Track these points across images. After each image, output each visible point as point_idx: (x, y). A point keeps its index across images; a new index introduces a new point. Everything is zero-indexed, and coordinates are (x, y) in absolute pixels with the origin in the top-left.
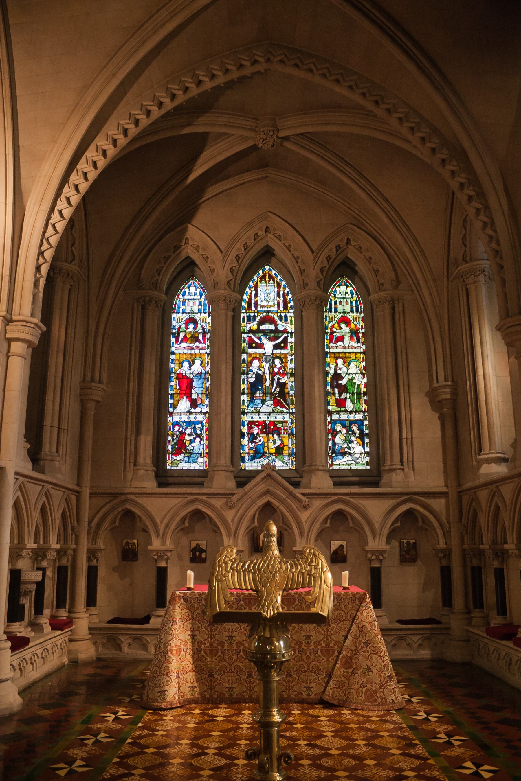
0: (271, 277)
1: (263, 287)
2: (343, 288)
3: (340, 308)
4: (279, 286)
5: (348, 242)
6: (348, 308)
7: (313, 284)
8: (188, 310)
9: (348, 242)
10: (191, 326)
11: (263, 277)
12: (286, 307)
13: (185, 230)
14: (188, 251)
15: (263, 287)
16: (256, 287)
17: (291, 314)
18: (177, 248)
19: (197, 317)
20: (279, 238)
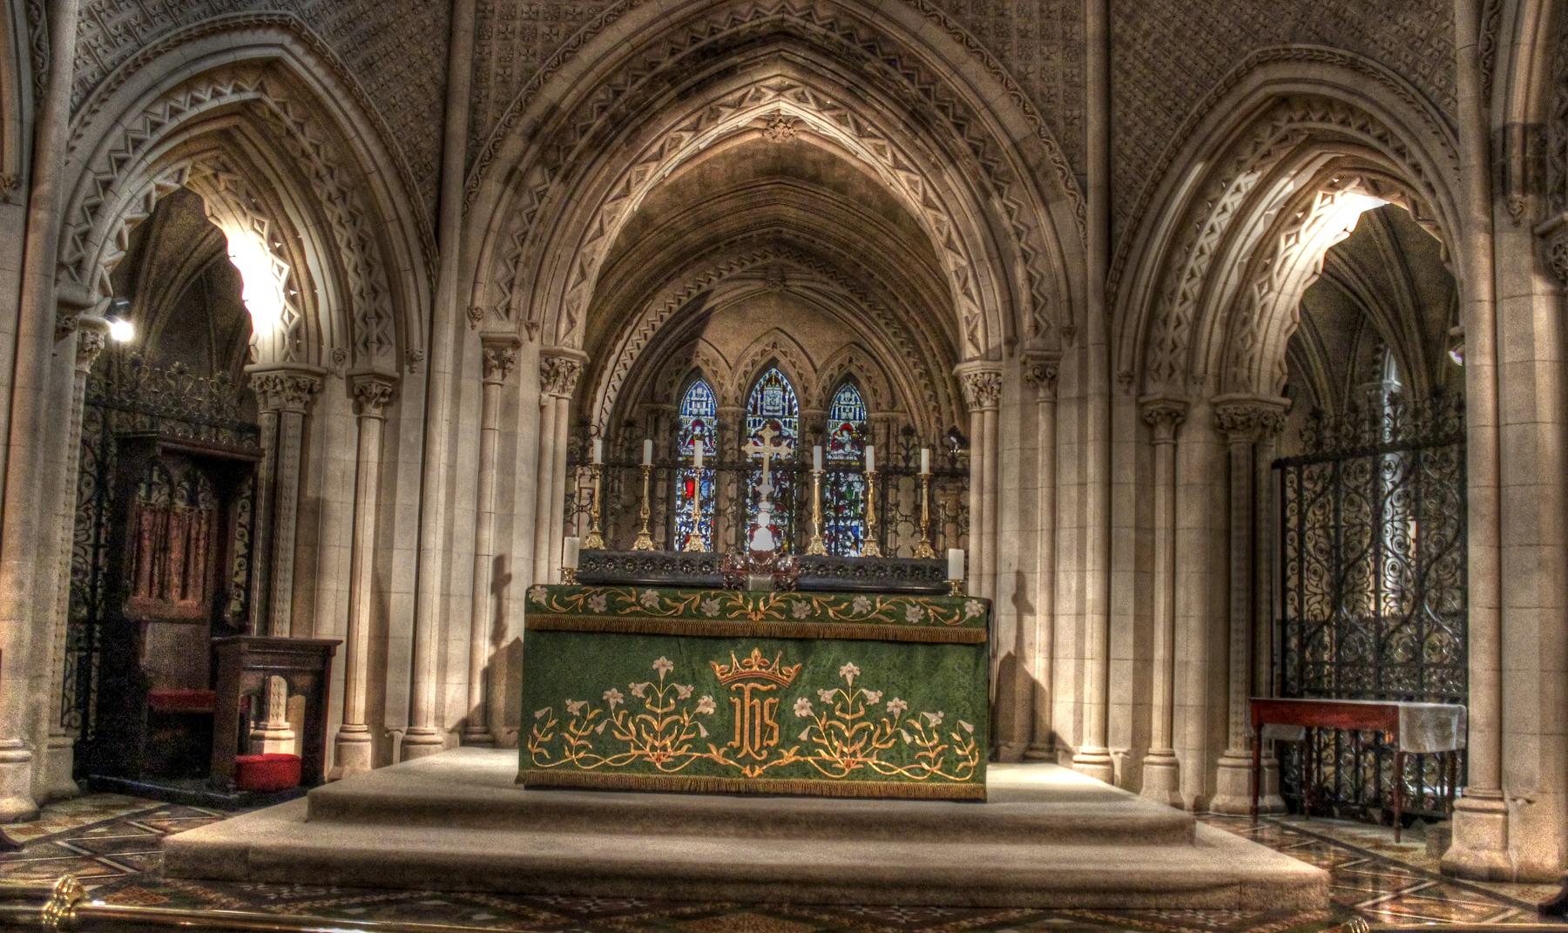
0: (777, 381)
1: (769, 390)
2: (848, 395)
3: (844, 415)
4: (784, 390)
5: (851, 361)
6: (851, 415)
7: (814, 403)
8: (695, 411)
9: (851, 361)
10: (698, 429)
11: (769, 380)
12: (790, 412)
13: (695, 345)
14: (697, 362)
15: (769, 390)
16: (762, 390)
17: (795, 420)
18: (688, 361)
19: (703, 419)
20: (785, 354)
